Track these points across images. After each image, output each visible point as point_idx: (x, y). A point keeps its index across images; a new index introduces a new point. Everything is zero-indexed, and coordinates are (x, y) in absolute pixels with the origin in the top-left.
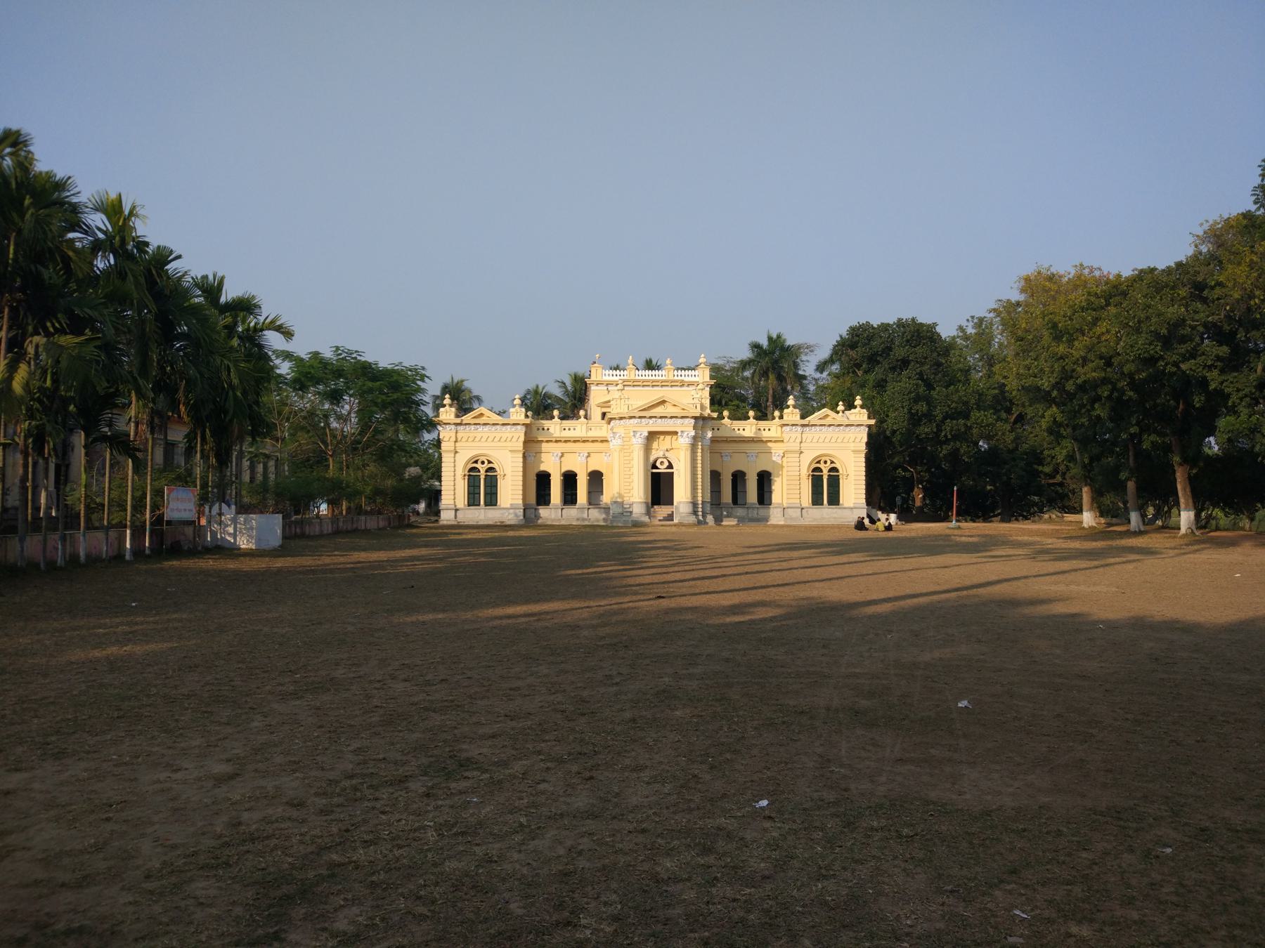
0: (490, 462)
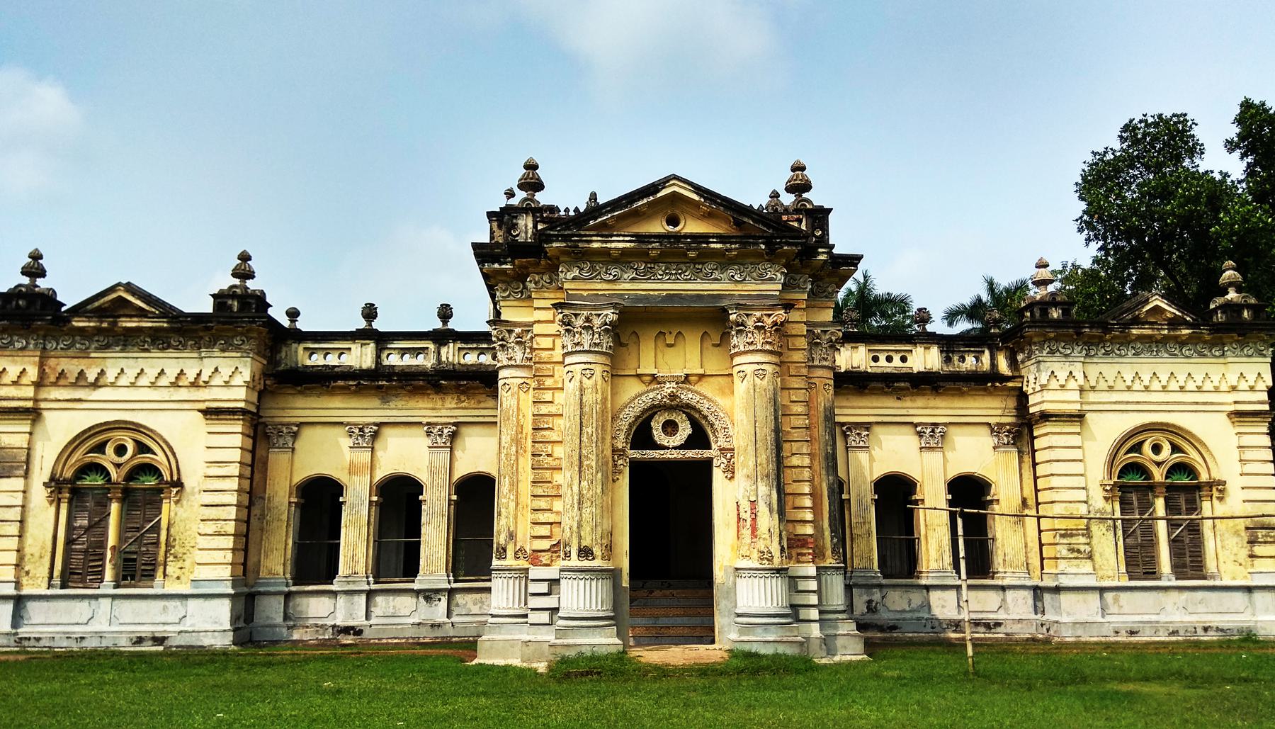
0: (142, 448)
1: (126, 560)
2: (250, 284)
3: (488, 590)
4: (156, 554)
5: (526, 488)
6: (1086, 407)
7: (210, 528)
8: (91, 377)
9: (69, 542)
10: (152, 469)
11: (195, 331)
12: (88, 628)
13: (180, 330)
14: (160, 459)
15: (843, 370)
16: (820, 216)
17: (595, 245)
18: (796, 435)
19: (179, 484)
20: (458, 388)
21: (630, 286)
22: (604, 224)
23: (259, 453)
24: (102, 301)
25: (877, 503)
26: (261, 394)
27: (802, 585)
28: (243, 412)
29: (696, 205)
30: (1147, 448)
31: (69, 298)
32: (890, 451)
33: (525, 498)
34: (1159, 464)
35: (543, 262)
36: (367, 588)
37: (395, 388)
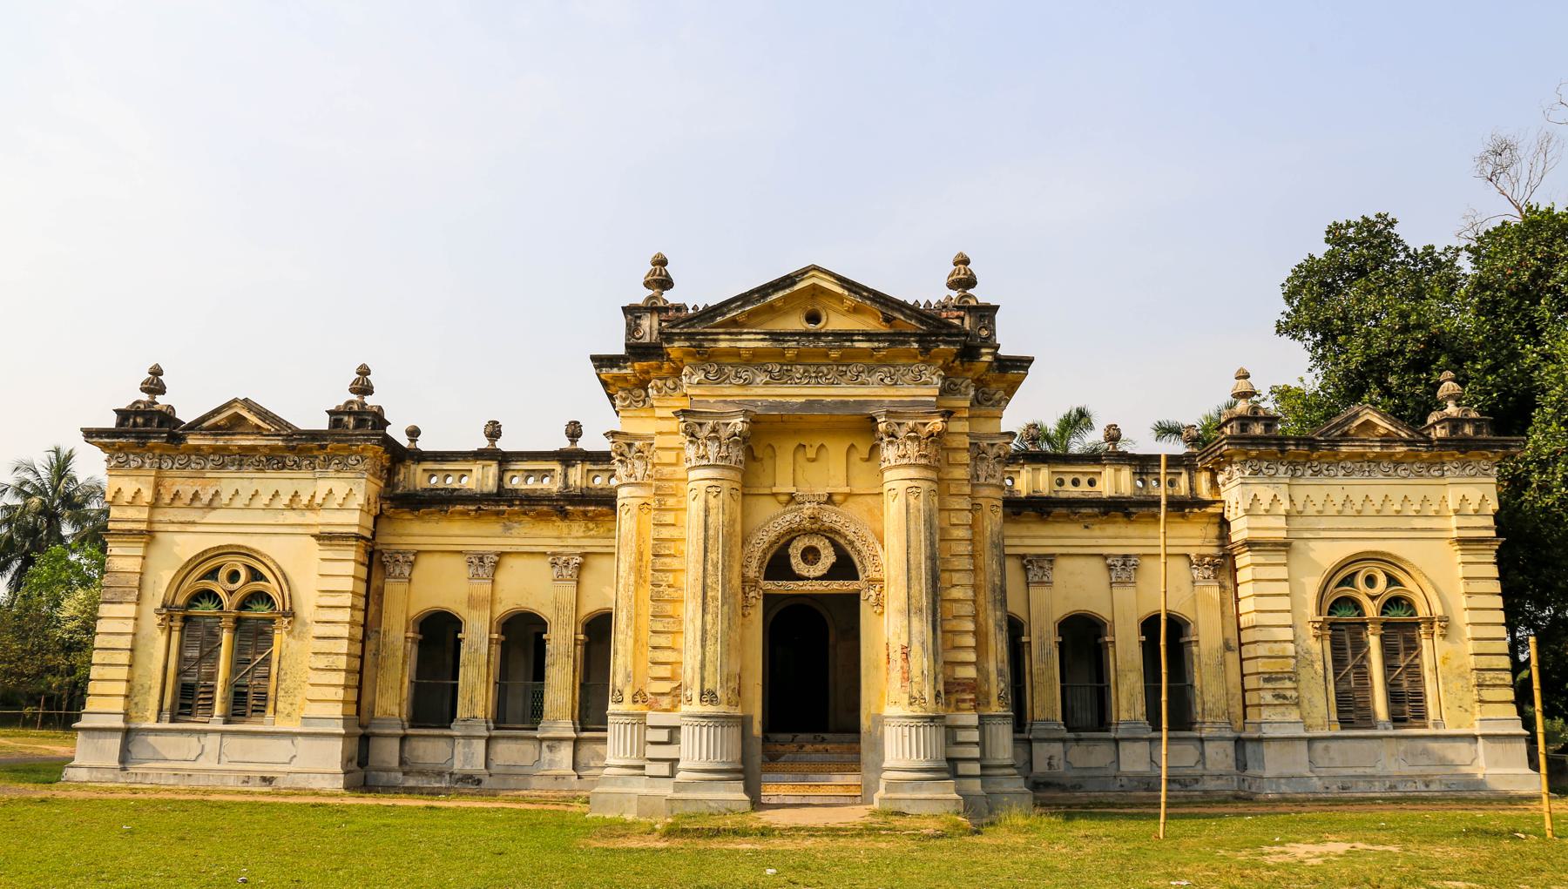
0: (255, 575)
1: (236, 694)
2: (370, 401)
3: (604, 740)
4: (266, 687)
5: (646, 622)
6: (1293, 534)
7: (322, 662)
8: (206, 499)
9: (180, 673)
10: (265, 598)
11: (311, 450)
12: (197, 765)
13: (298, 449)
14: (272, 588)
15: (1024, 494)
16: (986, 313)
17: (723, 345)
18: (958, 563)
19: (291, 614)
20: (585, 513)
21: (764, 392)
22: (734, 322)
23: (375, 583)
24: (218, 418)
25: (1062, 646)
26: (376, 518)
27: (962, 736)
28: (358, 537)
29: (840, 298)
30: (1360, 580)
31: (186, 415)
32: (1077, 585)
33: (645, 635)
34: (1373, 598)
35: (666, 365)
36: (486, 734)
37: (516, 513)
